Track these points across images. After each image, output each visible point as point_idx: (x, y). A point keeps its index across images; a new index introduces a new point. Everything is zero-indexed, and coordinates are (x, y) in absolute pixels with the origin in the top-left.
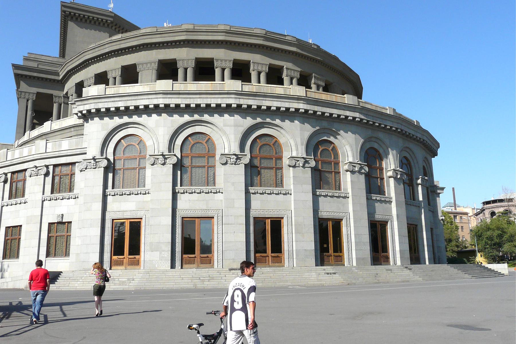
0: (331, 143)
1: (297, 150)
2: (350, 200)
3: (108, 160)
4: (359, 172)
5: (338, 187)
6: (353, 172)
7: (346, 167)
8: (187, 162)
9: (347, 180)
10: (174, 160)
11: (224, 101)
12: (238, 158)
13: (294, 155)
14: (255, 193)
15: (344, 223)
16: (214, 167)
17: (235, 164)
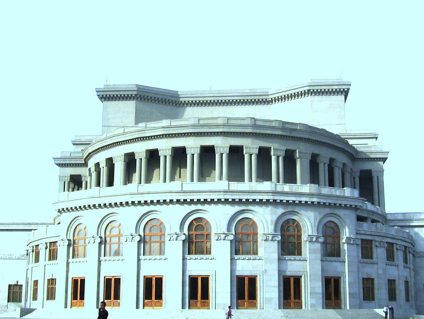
0: (294, 221)
2: (308, 262)
3: (140, 235)
4: (317, 241)
5: (300, 254)
6: (311, 241)
7: (305, 239)
9: (306, 248)
10: (183, 237)
11: (216, 197)
12: (227, 235)
14: (238, 259)
15: (303, 279)
17: (224, 239)
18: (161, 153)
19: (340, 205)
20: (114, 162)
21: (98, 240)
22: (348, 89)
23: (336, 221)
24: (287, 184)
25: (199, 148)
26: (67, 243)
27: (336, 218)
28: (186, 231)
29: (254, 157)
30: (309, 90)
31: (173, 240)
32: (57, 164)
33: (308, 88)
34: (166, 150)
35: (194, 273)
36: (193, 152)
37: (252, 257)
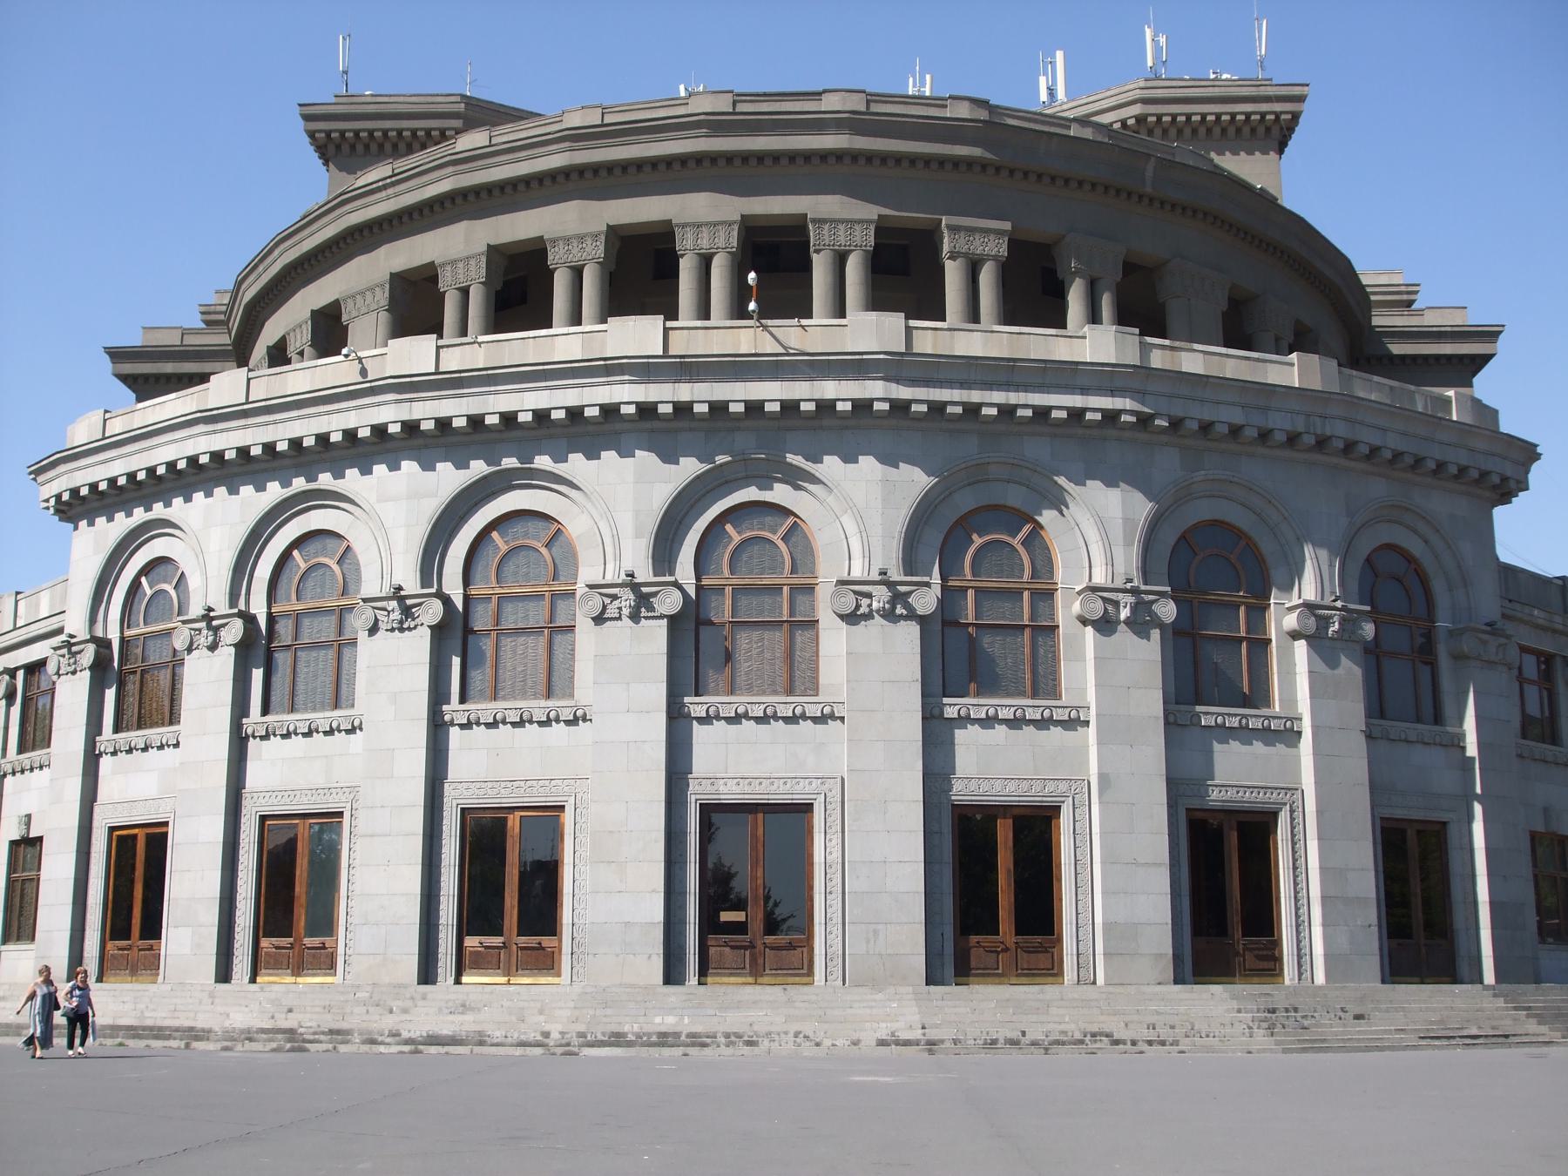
1: (1111, 562)
3: (447, 601)
8: (722, 610)
13: (1099, 578)
16: (813, 624)
18: (553, 257)
19: (1441, 466)
20: (344, 318)
21: (234, 631)
22: (1296, 117)
23: (1415, 547)
24: (1196, 346)
25: (736, 227)
26: (88, 655)
27: (1415, 532)
28: (685, 571)
29: (987, 277)
30: (1141, 119)
31: (620, 618)
32: (126, 379)
33: (1136, 110)
34: (581, 238)
35: (730, 792)
36: (705, 244)
37: (1033, 708)
